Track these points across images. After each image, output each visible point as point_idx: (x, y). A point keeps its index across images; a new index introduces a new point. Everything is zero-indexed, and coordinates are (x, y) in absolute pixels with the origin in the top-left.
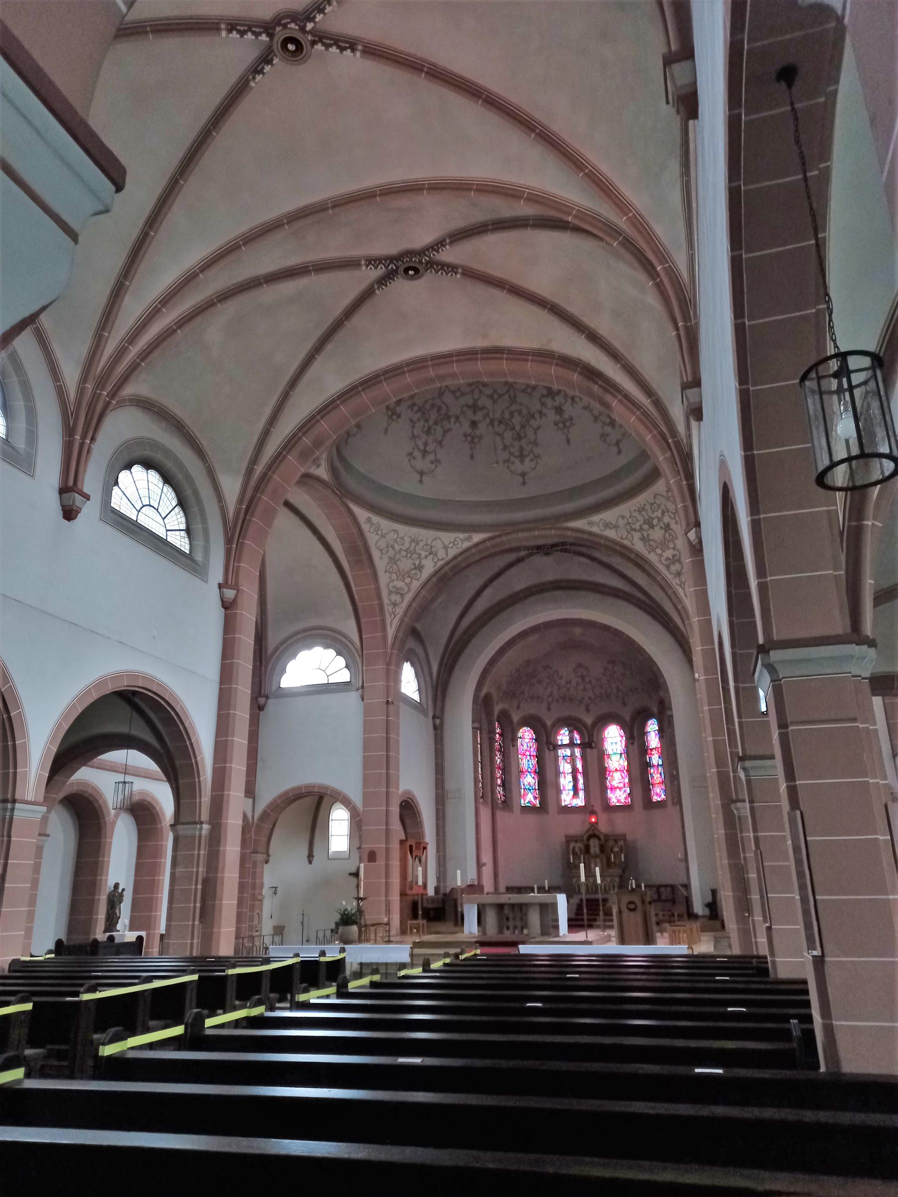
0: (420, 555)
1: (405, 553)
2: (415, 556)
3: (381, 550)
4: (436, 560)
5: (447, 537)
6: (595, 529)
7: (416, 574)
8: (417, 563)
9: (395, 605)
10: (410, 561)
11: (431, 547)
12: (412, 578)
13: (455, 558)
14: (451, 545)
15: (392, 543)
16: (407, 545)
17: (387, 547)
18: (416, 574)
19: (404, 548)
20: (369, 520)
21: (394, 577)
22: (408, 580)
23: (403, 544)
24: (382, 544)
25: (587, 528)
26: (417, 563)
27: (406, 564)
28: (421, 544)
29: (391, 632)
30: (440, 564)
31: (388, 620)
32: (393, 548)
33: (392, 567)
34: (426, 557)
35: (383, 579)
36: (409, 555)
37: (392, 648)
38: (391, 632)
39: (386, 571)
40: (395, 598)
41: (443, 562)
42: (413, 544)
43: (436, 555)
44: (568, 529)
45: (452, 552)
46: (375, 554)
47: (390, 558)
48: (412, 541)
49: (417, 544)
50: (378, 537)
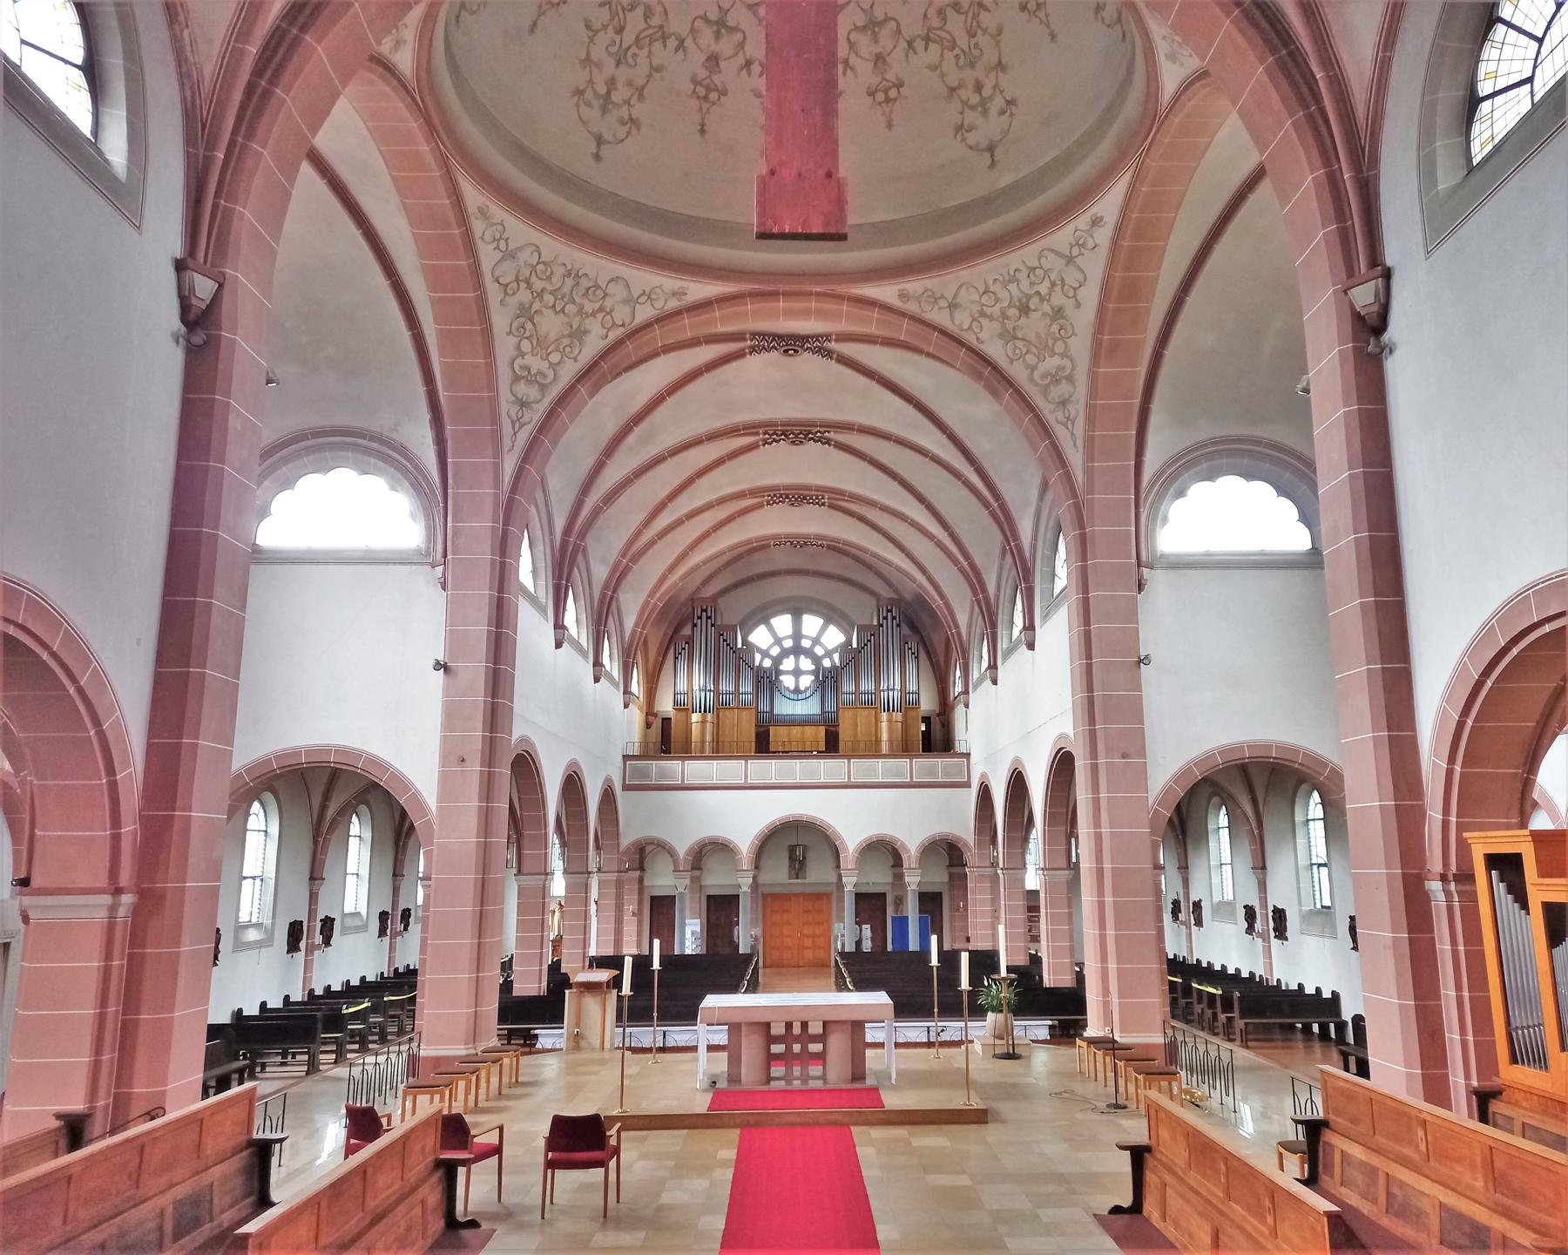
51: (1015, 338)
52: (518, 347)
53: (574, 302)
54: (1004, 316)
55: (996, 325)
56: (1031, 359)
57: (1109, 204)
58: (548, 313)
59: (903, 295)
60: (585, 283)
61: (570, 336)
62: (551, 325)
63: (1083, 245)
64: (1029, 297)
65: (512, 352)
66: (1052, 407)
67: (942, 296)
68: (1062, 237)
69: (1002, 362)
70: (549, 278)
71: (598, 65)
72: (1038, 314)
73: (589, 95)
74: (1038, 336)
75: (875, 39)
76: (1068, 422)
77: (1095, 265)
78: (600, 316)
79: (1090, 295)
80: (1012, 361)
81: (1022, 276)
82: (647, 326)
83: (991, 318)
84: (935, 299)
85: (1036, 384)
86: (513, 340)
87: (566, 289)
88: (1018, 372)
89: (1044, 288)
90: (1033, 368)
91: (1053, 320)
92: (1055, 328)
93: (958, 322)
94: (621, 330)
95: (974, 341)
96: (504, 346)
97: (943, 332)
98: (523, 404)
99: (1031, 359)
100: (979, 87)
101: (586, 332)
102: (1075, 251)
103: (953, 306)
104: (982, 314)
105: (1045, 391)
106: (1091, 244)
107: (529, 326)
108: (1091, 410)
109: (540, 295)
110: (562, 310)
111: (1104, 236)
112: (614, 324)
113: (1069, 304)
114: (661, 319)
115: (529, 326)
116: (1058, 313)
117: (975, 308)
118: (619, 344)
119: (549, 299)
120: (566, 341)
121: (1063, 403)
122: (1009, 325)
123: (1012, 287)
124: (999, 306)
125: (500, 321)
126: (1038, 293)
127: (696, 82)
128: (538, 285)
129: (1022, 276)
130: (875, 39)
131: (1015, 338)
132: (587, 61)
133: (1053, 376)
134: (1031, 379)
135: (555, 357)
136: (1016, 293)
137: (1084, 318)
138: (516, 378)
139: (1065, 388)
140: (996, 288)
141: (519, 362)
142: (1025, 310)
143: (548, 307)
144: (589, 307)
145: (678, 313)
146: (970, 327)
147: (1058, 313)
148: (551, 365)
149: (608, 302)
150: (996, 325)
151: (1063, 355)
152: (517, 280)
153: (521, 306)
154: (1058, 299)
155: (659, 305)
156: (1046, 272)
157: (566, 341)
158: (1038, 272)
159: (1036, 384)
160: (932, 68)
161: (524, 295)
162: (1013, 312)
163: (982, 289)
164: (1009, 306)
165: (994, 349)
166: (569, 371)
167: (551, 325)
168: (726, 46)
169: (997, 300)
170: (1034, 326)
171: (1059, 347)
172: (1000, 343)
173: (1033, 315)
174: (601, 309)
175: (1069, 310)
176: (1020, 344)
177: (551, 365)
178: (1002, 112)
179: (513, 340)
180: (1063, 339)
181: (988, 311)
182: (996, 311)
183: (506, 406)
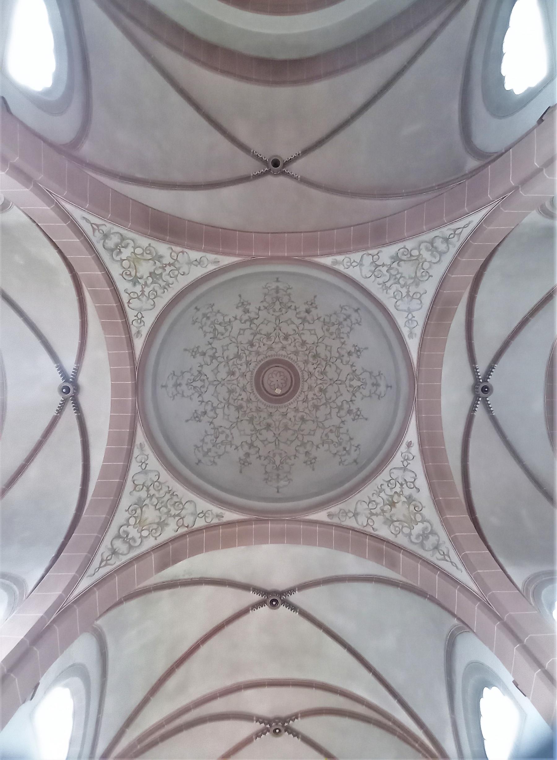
1: (402, 281)
2: (393, 272)
3: (419, 299)
4: (376, 257)
5: (354, 273)
6: (212, 257)
7: (403, 254)
8: (395, 265)
9: (446, 240)
10: (401, 270)
12: (410, 252)
13: (357, 250)
14: (354, 264)
16: (394, 287)
17: (412, 298)
18: (403, 254)
19: (398, 286)
20: (411, 335)
22: (415, 253)
23: (397, 290)
24: (415, 304)
25: (219, 257)
27: (407, 269)
28: (381, 280)
29: (476, 218)
30: (374, 252)
31: (466, 232)
32: (408, 292)
33: (422, 276)
34: (383, 265)
35: (438, 271)
36: (398, 276)
37: (489, 202)
38: (476, 218)
41: (370, 252)
43: (373, 262)
44: (239, 255)
45: (356, 256)
46: (427, 300)
47: (417, 285)
50: (414, 314)
51: (393, 521)
52: (128, 520)
53: (166, 507)
54: (383, 511)
56: (406, 530)
57: (412, 434)
58: (152, 508)
59: (330, 515)
60: (175, 499)
61: (158, 524)
62: (150, 514)
63: (408, 459)
64: (392, 497)
65: (123, 521)
66: (431, 552)
67: (350, 511)
69: (391, 538)
70: (159, 490)
71: (207, 443)
72: (400, 503)
73: (200, 449)
74: (404, 516)
75: (305, 448)
76: (445, 556)
77: (417, 466)
78: (177, 518)
79: (422, 482)
81: (385, 487)
82: (200, 530)
83: (377, 515)
84: (345, 513)
85: (415, 544)
86: (127, 515)
87: (165, 499)
88: (402, 540)
89: (398, 489)
90: (410, 535)
91: (409, 504)
92: (412, 508)
93: (359, 523)
94: (186, 529)
95: (372, 531)
96: (121, 516)
97: (354, 530)
98: (114, 552)
99: (406, 530)
100: (345, 449)
101: (167, 524)
103: (356, 515)
104: (372, 514)
105: (422, 545)
107: (139, 511)
108: (455, 542)
109: (151, 497)
110: (159, 509)
111: (415, 450)
112: (183, 525)
114: (209, 528)
115: (139, 511)
118: (183, 536)
119: (155, 501)
120: (155, 526)
123: (382, 494)
124: (379, 506)
125: (126, 501)
126: (396, 492)
127: (240, 459)
128: (152, 492)
129: (385, 487)
130: (305, 448)
131: (393, 521)
132: (203, 440)
135: (145, 533)
136: (385, 497)
137: (424, 495)
138: (118, 536)
140: (375, 498)
141: (124, 528)
142: (393, 504)
143: (152, 505)
144: (173, 512)
145: (216, 526)
146: (368, 524)
147: (410, 499)
148: (141, 537)
149: (184, 513)
150: (381, 518)
151: (423, 521)
152: (143, 485)
153: (140, 499)
154: (407, 491)
155: (209, 520)
157: (155, 526)
159: (415, 544)
160: (326, 451)
161: (143, 494)
162: (387, 508)
163: (367, 501)
164: (384, 505)
165: (384, 532)
166: (151, 543)
167: (150, 514)
168: (252, 451)
169: (377, 504)
170: (401, 511)
172: (386, 527)
173: (397, 505)
174: (178, 515)
175: (415, 495)
176: (397, 524)
177: (141, 537)
178: (356, 450)
179: (127, 515)
182: (378, 510)
183: (104, 549)
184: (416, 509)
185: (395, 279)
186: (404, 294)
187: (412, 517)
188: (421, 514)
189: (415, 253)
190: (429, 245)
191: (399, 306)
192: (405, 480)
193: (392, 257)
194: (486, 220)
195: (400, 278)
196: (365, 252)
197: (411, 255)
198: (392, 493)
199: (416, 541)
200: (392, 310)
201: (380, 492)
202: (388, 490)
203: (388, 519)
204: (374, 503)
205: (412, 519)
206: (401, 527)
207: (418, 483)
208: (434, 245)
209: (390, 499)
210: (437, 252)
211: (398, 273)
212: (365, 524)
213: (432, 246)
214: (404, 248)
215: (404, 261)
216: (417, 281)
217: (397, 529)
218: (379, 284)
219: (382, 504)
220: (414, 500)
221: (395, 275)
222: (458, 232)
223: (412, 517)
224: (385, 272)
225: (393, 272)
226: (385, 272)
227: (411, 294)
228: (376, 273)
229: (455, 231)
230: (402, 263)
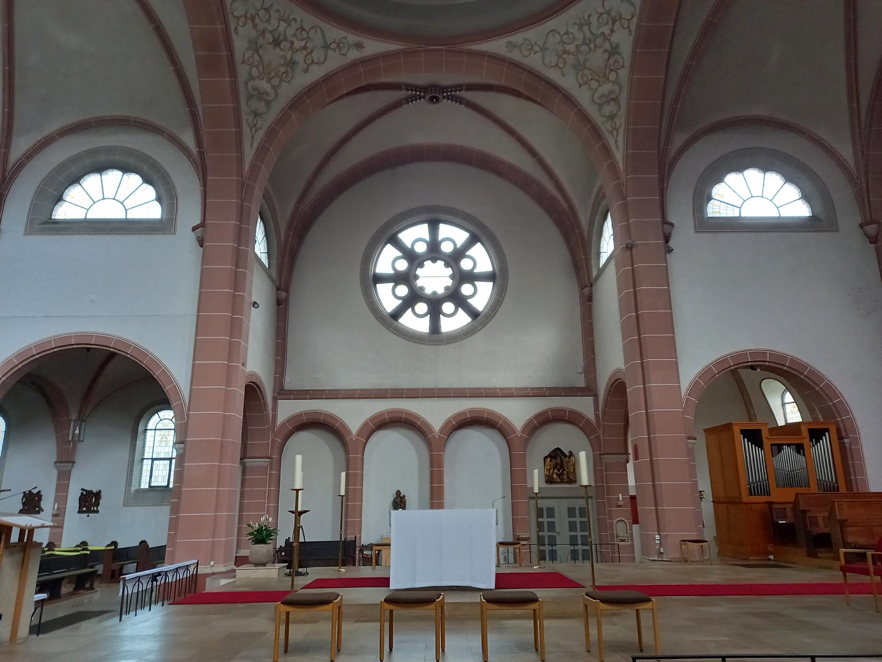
0: (603, 33)
1: (584, 48)
2: (599, 41)
8: (607, 46)
9: (612, 117)
10: (599, 51)
11: (608, 13)
12: (615, 70)
15: (560, 48)
16: (580, 36)
17: (559, 57)
21: (594, 84)
22: (612, 76)
23: (574, 39)
24: (551, 58)
26: (607, 46)
27: (597, 59)
28: (594, 19)
29: (619, 156)
31: (611, 141)
32: (569, 53)
33: (583, 76)
34: (612, 31)
35: (583, 97)
36: (592, 46)
38: (619, 156)
39: (580, 86)
40: (608, 109)
41: (635, 19)
42: (586, 29)
43: (621, 18)
46: (554, 75)
47: (575, 67)
48: (581, 26)
49: (589, 24)
54: (263, 33)
55: (254, 34)
57: (374, 47)
64: (285, 39)
68: (335, 33)
69: (238, 57)
72: (282, 53)
77: (334, 61)
79: (317, 73)
80: (243, 62)
81: (295, 26)
83: (255, 26)
88: (242, 71)
89: (298, 44)
90: (252, 78)
92: (283, 69)
95: (232, 28)
99: (255, 71)
102: (333, 46)
104: (253, 19)
105: (249, 97)
106: (344, 51)
111: (354, 55)
113: (302, 65)
116: (292, 63)
117: (252, 11)
121: (256, 114)
122: (261, 41)
123: (283, 25)
124: (265, 25)
126: (292, 43)
129: (295, 26)
133: (259, 92)
134: (247, 84)
137: (303, 80)
139: (261, 106)
140: (274, 15)
142: (277, 43)
146: (238, 18)
147: (292, 63)
150: (254, 34)
151: (273, 87)
154: (299, 57)
156: (308, 39)
158: (304, 33)
163: (267, 6)
164: (271, 32)
165: (240, 45)
169: (268, 21)
170: (274, 56)
171: (275, 81)
173: (278, 50)
176: (256, 57)
180: (281, 80)
181: (257, 20)
182: (262, 26)
184: (284, 75)
185: (590, 40)
186: (567, 47)
187: (273, 74)
188: (280, 82)
189: (612, 76)
190: (614, 96)
191: (554, 36)
192: (312, 52)
193: (617, 46)
194: (613, 166)
195: (590, 48)
196: (638, 10)
197: (611, 71)
198: (290, 39)
199: (250, 88)
200: (551, 24)
201: (285, 20)
202: (290, 31)
203: (256, 43)
204: (267, 17)
205: (270, 74)
206: (256, 63)
207: (314, 68)
208: (613, 102)
209: (281, 38)
210: (604, 103)
211: (596, 46)
212: (236, 14)
213: (612, 99)
214: (623, 66)
215: (608, 60)
216: (579, 67)
217: (251, 60)
218: (589, 16)
219: (270, 29)
220: (292, 70)
221: (595, 41)
222: (615, 132)
223: (273, 74)
224: (602, 29)
225: (599, 41)
226: (602, 29)
227: (565, 56)
228: (605, 16)
229: (617, 130)
230: (606, 56)
